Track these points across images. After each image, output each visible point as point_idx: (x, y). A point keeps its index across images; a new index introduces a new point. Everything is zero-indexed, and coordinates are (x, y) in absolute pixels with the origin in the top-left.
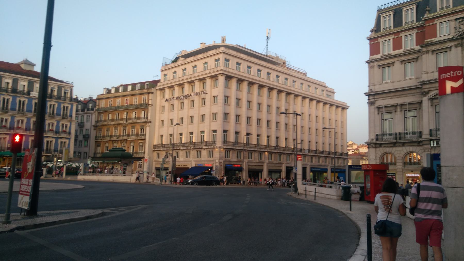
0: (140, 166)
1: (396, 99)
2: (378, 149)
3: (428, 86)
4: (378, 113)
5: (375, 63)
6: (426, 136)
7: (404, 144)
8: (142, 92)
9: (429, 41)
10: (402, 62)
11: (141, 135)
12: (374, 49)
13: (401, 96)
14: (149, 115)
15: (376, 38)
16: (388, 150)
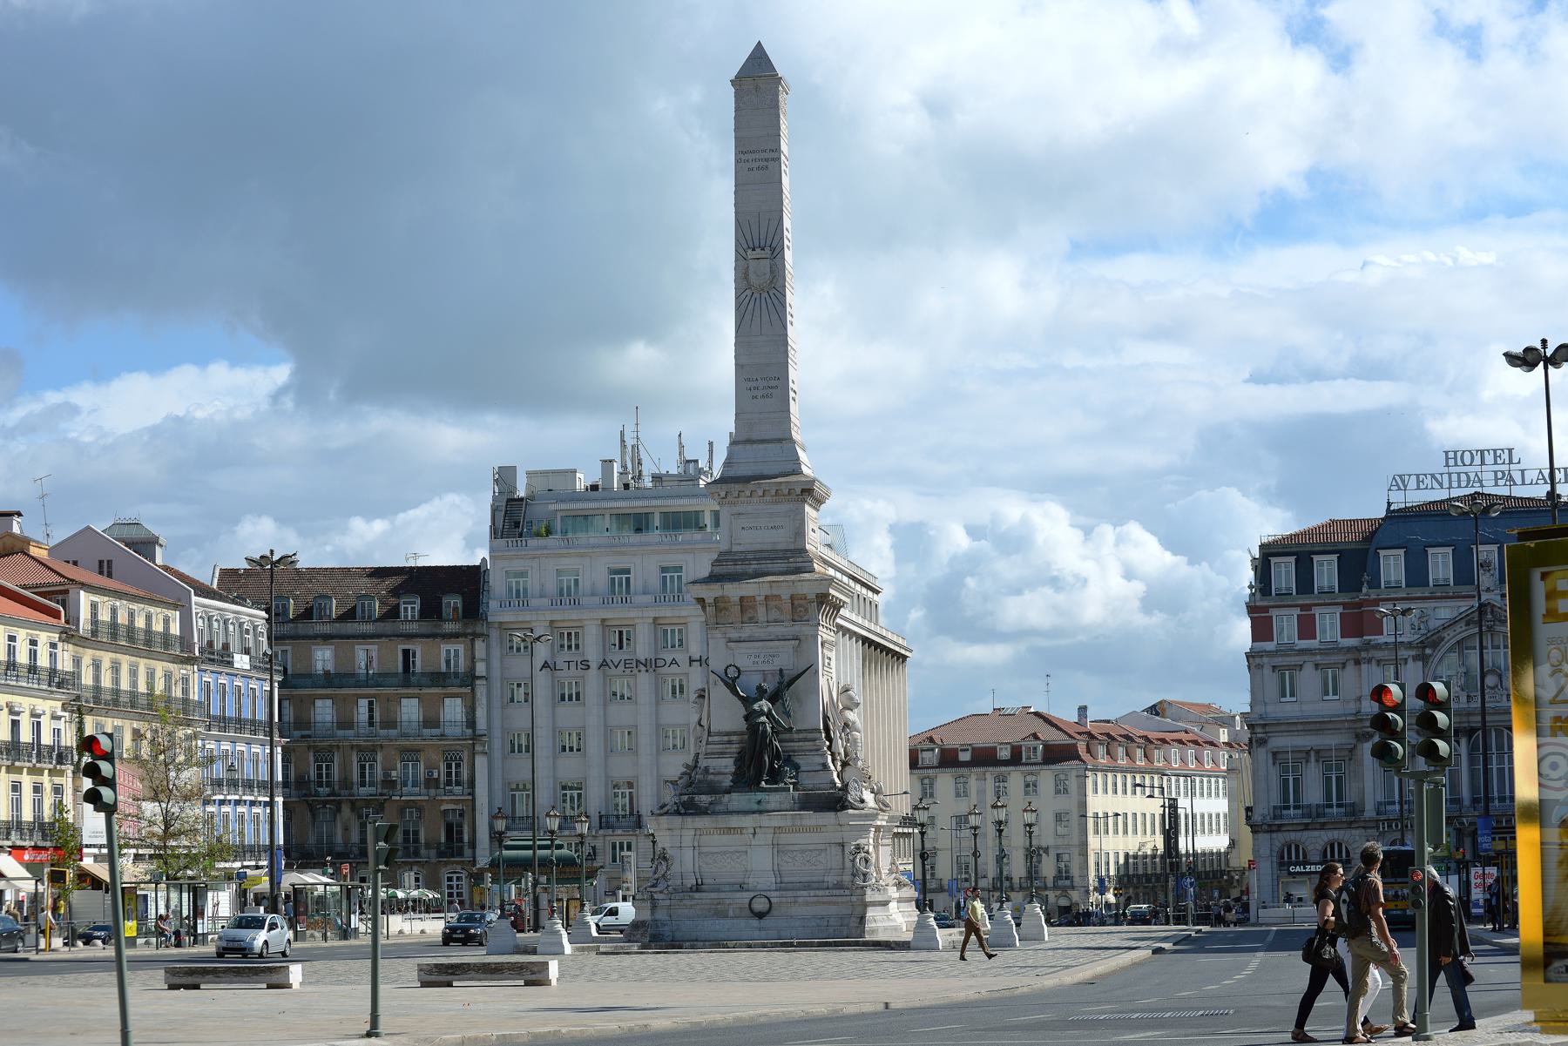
0: (454, 883)
1: (1308, 738)
2: (1274, 835)
4: (1274, 764)
5: (1265, 660)
6: (1370, 812)
7: (1323, 827)
9: (1370, 640)
10: (1317, 666)
11: (449, 783)
12: (1261, 630)
14: (481, 713)
15: (1266, 609)
16: (1293, 836)
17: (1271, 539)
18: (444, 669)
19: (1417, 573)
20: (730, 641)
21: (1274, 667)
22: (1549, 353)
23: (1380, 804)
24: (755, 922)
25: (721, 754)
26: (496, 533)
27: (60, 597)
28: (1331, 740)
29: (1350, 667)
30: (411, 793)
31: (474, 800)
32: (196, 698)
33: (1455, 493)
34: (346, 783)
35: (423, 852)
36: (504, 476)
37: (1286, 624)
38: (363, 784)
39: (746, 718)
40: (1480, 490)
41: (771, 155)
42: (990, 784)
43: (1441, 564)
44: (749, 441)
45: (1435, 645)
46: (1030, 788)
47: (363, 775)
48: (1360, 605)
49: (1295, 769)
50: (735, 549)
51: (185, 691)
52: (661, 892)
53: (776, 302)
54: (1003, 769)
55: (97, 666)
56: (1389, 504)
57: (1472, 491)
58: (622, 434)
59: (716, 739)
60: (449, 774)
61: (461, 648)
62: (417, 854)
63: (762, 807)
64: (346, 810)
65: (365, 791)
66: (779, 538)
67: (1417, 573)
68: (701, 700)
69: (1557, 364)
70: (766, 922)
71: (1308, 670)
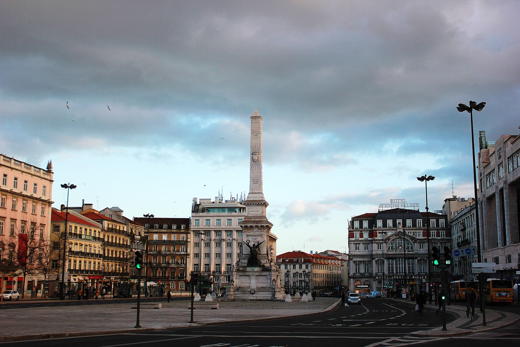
3: (375, 256)
4: (354, 264)
5: (353, 242)
7: (364, 278)
8: (179, 232)
10: (363, 244)
13: (363, 257)
15: (353, 231)
17: (354, 217)
18: (181, 240)
19: (385, 225)
20: (248, 235)
21: (354, 244)
22: (427, 178)
23: (376, 273)
24: (251, 295)
25: (245, 259)
26: (193, 212)
27: (101, 222)
28: (366, 259)
29: (370, 244)
30: (173, 266)
31: (186, 267)
32: (129, 244)
33: (393, 208)
34: (160, 263)
35: (175, 278)
36: (195, 200)
37: (357, 234)
38: (163, 263)
39: (250, 251)
40: (398, 208)
41: (259, 133)
42: (292, 266)
43: (390, 222)
44: (252, 193)
45: (388, 240)
46: (301, 267)
47: (163, 262)
48: (373, 231)
49: (359, 265)
50: (249, 215)
51: (127, 243)
52: (231, 288)
53: (259, 164)
54: (295, 263)
55: (108, 237)
56: (379, 210)
57: (396, 208)
58: (219, 192)
59: (244, 256)
60: (181, 262)
61: (185, 235)
62: (174, 278)
63: (253, 271)
64: (159, 269)
65: (163, 265)
66: (259, 213)
67: (385, 225)
68: (241, 247)
69: (428, 180)
70: (254, 295)
71: (361, 244)
